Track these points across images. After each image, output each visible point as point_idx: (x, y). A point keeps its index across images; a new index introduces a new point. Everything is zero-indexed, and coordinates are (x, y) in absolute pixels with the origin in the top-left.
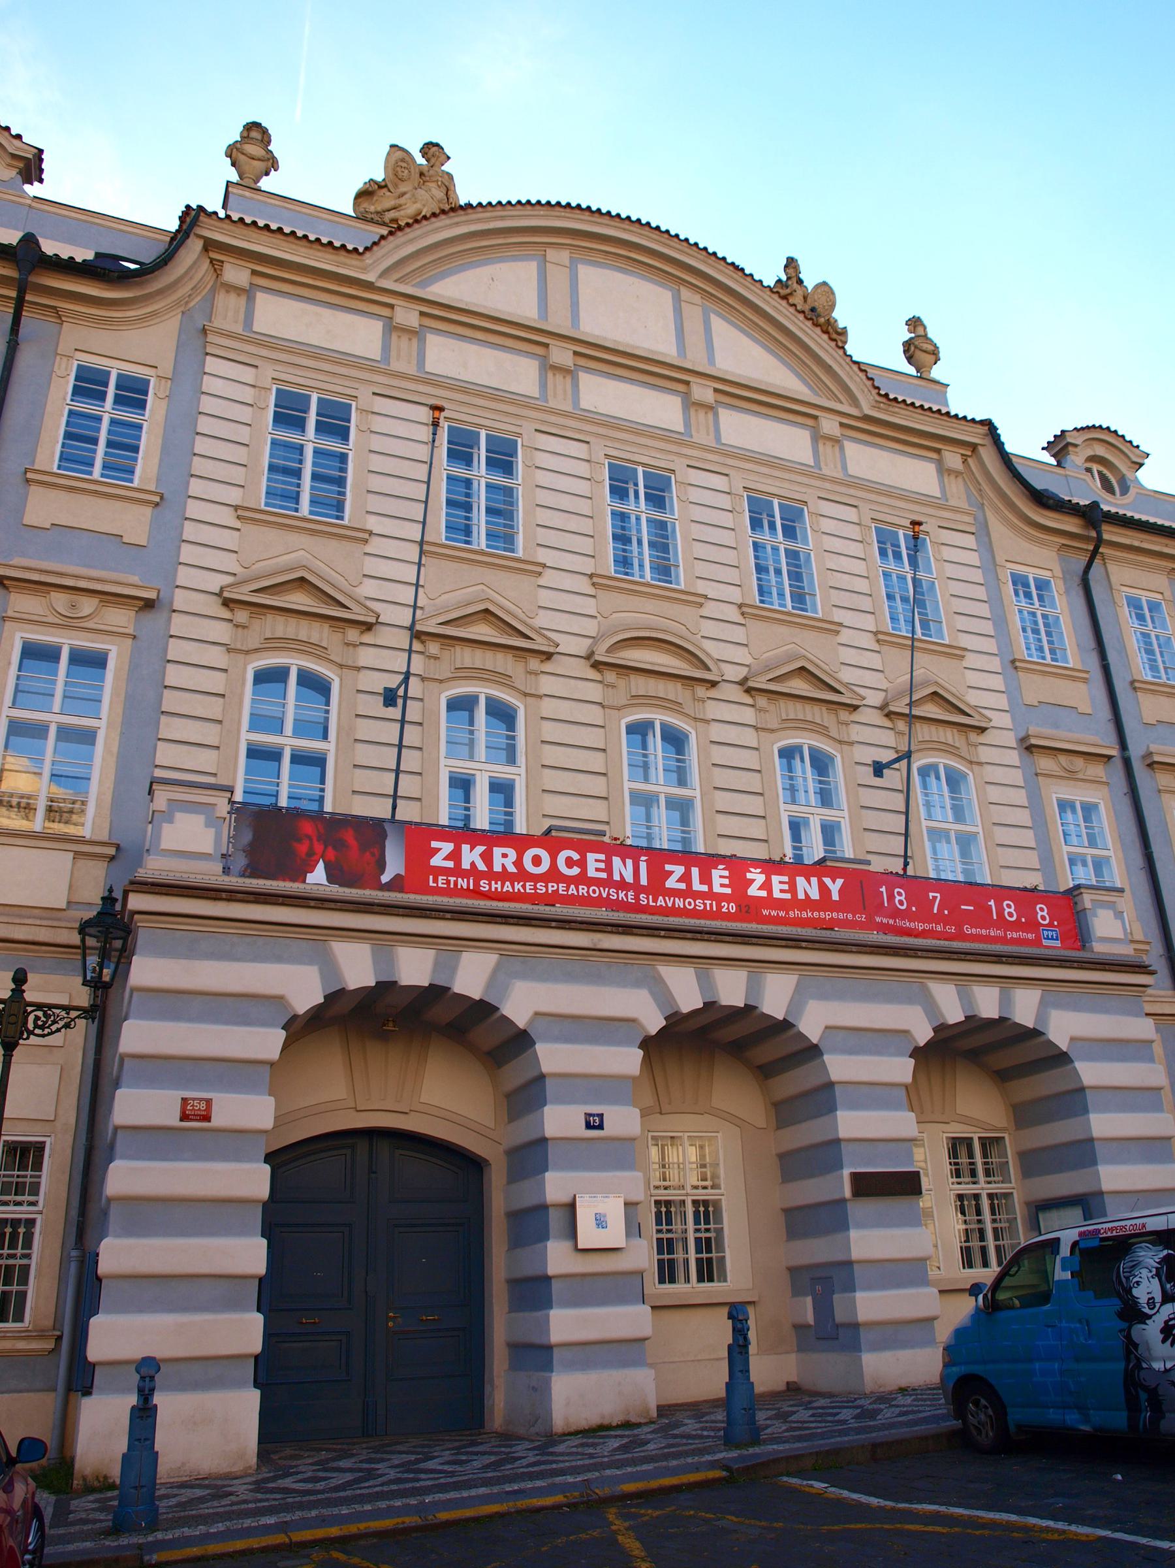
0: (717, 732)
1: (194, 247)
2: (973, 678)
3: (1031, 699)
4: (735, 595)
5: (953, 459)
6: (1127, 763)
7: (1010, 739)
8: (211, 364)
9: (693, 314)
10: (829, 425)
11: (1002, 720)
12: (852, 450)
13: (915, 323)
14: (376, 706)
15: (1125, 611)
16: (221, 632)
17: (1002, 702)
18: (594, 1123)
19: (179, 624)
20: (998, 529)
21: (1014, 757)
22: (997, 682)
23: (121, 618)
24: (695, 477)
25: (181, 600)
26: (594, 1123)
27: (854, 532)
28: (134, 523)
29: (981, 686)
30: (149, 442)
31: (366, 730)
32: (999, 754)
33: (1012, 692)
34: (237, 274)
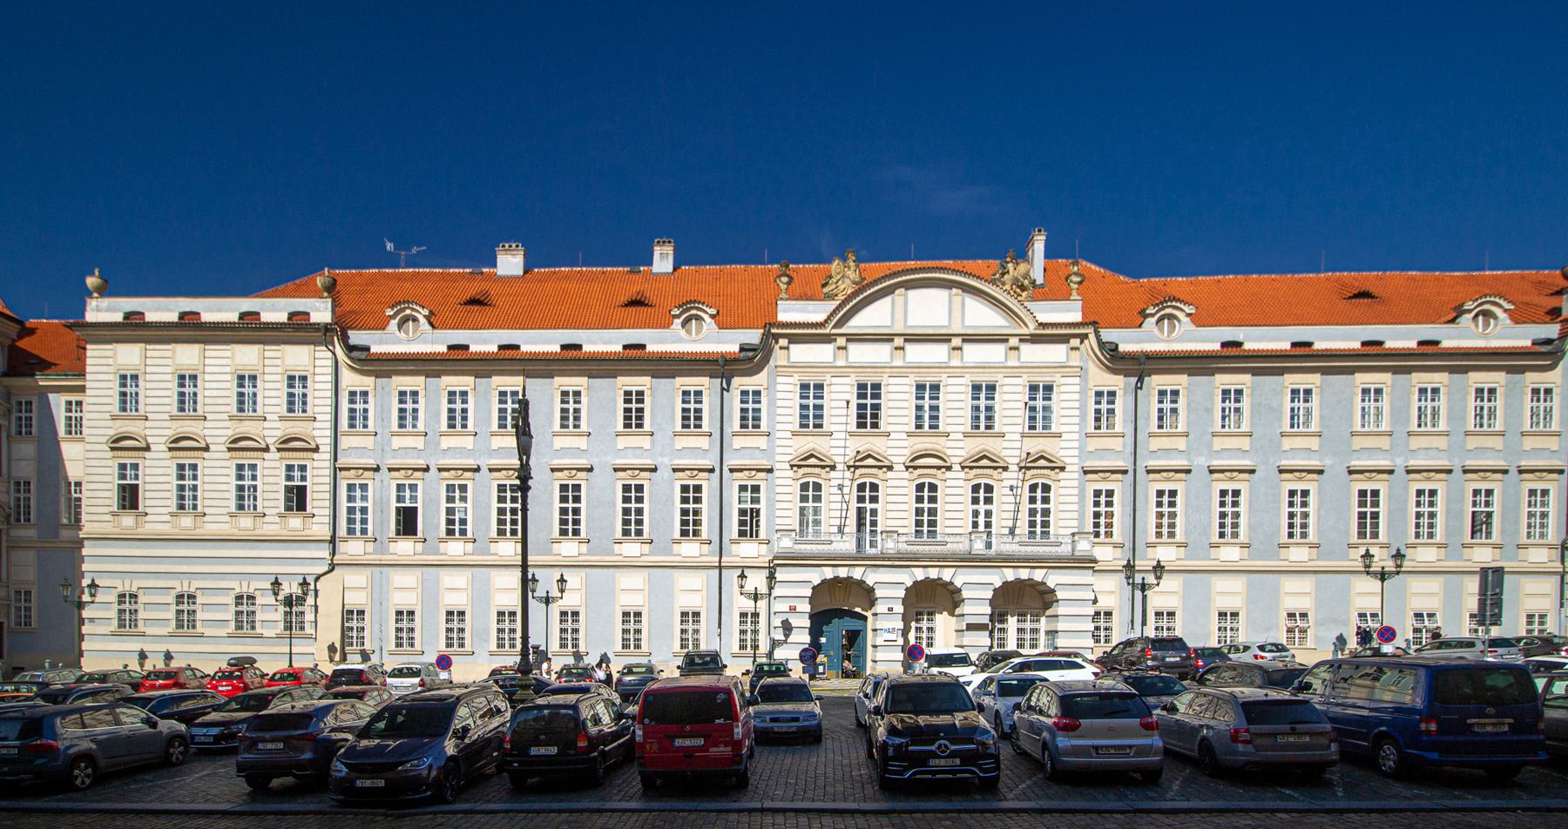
0: (949, 483)
2: (1063, 444)
3: (1091, 448)
4: (962, 428)
7: (1076, 468)
9: (957, 300)
10: (1014, 341)
11: (1076, 460)
16: (790, 473)
17: (1076, 452)
19: (777, 473)
21: (1076, 475)
23: (762, 475)
24: (951, 381)
25: (777, 466)
29: (1067, 449)
30: (764, 415)
31: (833, 498)
34: (783, 342)
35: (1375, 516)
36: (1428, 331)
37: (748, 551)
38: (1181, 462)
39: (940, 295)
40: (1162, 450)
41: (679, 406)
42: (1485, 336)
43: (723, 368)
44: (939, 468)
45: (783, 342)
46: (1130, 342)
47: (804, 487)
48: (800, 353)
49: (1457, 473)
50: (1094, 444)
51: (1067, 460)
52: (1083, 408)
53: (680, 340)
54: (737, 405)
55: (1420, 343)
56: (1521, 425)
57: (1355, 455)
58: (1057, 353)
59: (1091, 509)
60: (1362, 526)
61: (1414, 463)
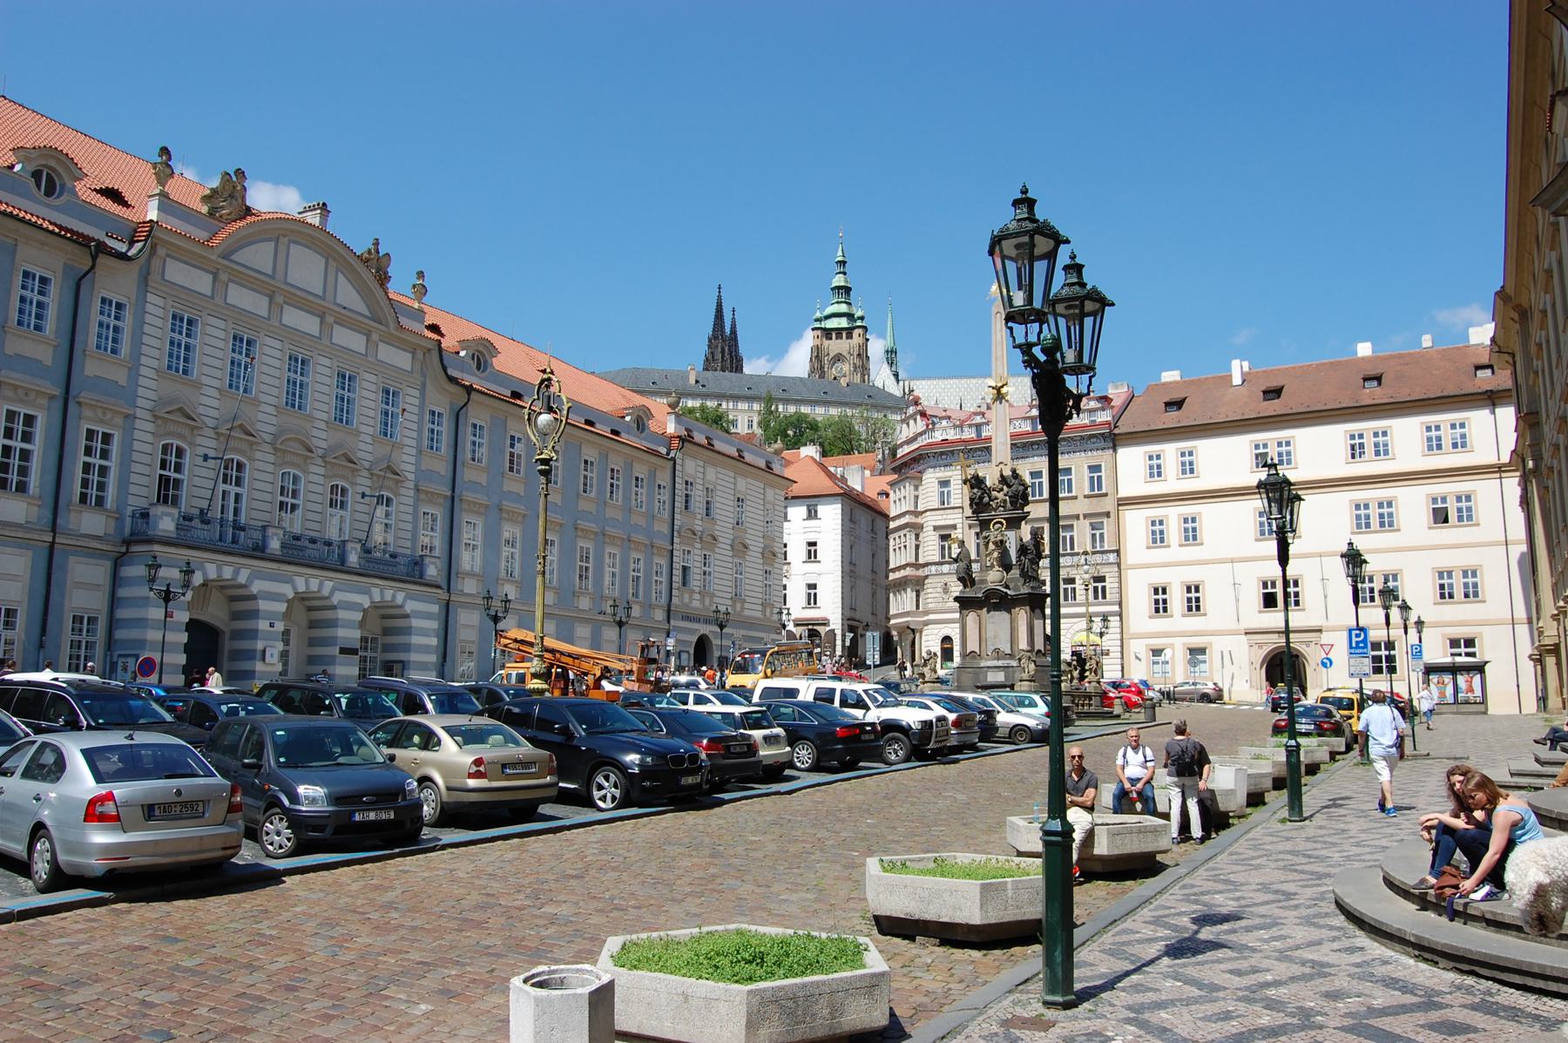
2: (405, 458)
5: (420, 355)
7: (411, 485)
8: (150, 297)
11: (411, 477)
12: (381, 345)
13: (421, 275)
14: (200, 461)
15: (470, 429)
16: (150, 427)
17: (412, 468)
18: (272, 625)
20: (429, 387)
21: (411, 493)
22: (413, 460)
26: (272, 625)
27: (373, 388)
28: (121, 376)
29: (407, 463)
30: (126, 337)
32: (407, 495)
33: (417, 464)
37: (91, 523)
41: (17, 292)
47: (165, 448)
48: (176, 272)
52: (420, 423)
54: (95, 317)
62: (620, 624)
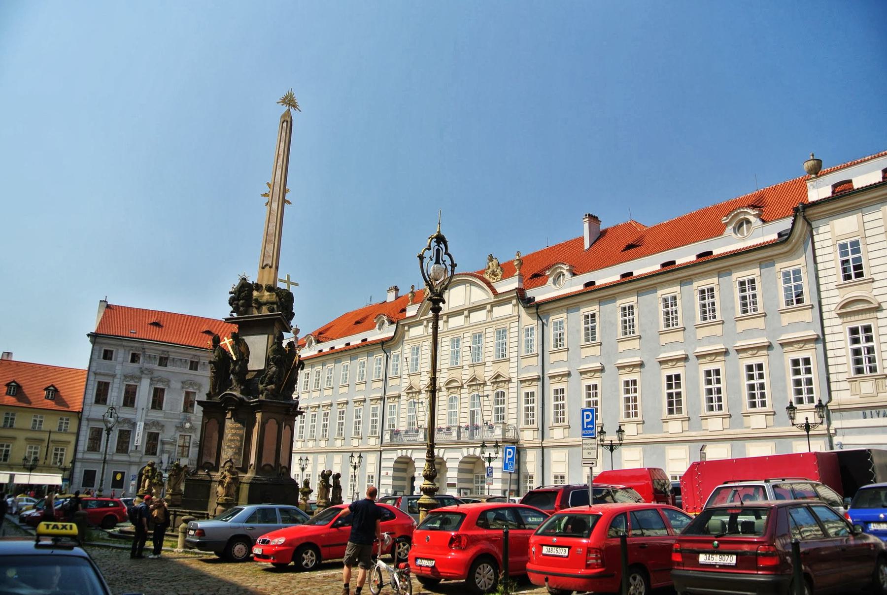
1: (400, 327)
6: (543, 378)
11: (516, 375)
21: (516, 384)
35: (679, 394)
36: (702, 246)
38: (564, 369)
39: (461, 288)
40: (557, 363)
42: (744, 239)
43: (385, 345)
44: (457, 387)
45: (406, 328)
46: (539, 294)
49: (733, 353)
50: (525, 363)
51: (512, 375)
53: (377, 334)
55: (699, 256)
56: (778, 306)
57: (663, 349)
58: (507, 310)
59: (524, 405)
60: (670, 404)
61: (700, 350)
62: (612, 447)
